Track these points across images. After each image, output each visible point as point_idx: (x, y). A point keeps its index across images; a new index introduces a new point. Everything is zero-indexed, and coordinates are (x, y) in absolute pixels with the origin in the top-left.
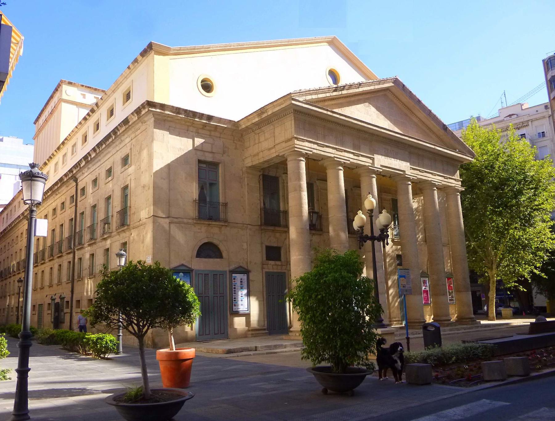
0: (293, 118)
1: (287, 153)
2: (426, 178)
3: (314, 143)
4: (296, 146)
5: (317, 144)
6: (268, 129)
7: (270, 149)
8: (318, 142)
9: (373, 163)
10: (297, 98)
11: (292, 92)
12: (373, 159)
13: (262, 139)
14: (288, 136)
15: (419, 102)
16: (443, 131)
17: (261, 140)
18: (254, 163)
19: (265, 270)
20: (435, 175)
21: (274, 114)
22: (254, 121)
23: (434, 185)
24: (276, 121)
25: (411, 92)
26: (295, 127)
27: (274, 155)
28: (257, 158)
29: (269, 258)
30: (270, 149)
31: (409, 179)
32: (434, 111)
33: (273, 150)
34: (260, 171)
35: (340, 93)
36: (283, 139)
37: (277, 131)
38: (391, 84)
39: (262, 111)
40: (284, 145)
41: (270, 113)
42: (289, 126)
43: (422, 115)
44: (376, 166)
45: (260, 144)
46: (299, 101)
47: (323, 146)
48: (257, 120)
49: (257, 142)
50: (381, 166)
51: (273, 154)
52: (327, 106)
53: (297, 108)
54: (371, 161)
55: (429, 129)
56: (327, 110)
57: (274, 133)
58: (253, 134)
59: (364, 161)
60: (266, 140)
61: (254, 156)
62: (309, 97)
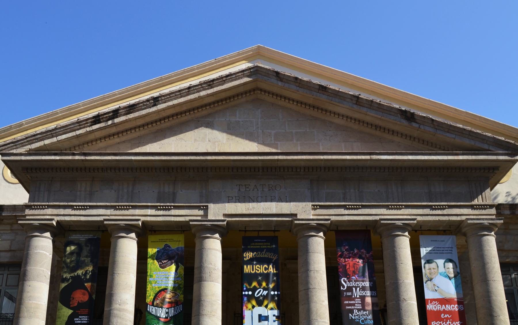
3: (65, 207)
4: (27, 217)
5: (72, 207)
9: (206, 215)
10: (14, 151)
16: (405, 122)
20: (399, 208)
35: (110, 122)
43: (343, 109)
44: (210, 217)
47: (85, 208)
50: (225, 215)
52: (106, 148)
54: (201, 212)
55: (377, 127)
56: (74, 154)
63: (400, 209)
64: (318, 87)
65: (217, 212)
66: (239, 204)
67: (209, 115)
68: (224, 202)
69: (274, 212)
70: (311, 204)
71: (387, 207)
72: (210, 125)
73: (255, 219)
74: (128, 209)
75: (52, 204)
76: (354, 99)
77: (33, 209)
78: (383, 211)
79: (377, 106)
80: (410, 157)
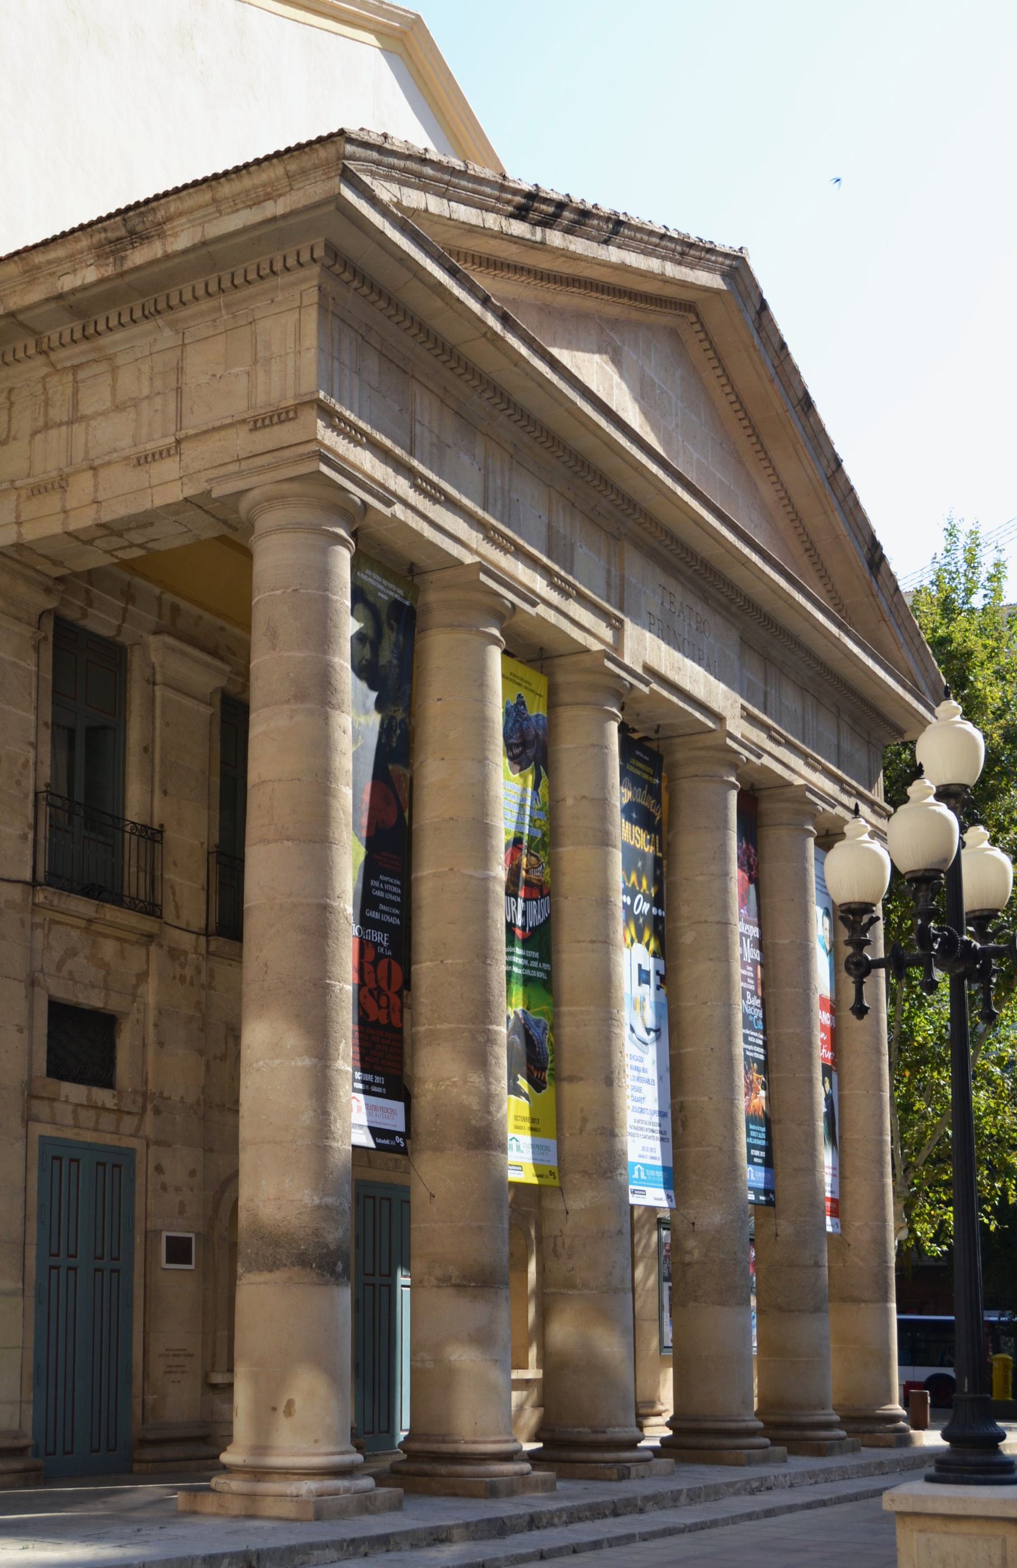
0: (313, 296)
1: (261, 484)
2: (786, 774)
6: (138, 353)
7: (143, 460)
8: (415, 463)
9: (618, 644)
11: (352, 127)
12: (618, 628)
13: (95, 398)
14: (276, 387)
15: (806, 404)
16: (867, 573)
17: (87, 407)
18: (30, 534)
19: (41, 1129)
21: (208, 256)
22: (68, 283)
23: (813, 814)
24: (204, 305)
25: (783, 346)
26: (320, 349)
27: (175, 494)
28: (53, 502)
29: (60, 1068)
30: (143, 460)
31: (734, 763)
32: (850, 469)
33: (169, 468)
34: (48, 591)
36: (239, 407)
37: (200, 364)
38: (713, 280)
39: (134, 223)
40: (242, 441)
41: (182, 241)
42: (287, 340)
45: (79, 429)
46: (373, 200)
48: (91, 275)
49: (59, 412)
51: (167, 485)
53: (351, 244)
54: (608, 634)
57: (180, 370)
58: (38, 368)
59: (584, 627)
60: (118, 408)
61: (37, 491)
62: (414, 198)
63: (815, 769)
64: (800, 395)
65: (644, 648)
66: (664, 646)
67: (615, 323)
68: (644, 627)
69: (699, 692)
70: (742, 701)
71: (805, 756)
72: (617, 361)
73: (674, 699)
74: (506, 551)
75: (379, 436)
76: (833, 466)
77: (334, 428)
78: (797, 763)
79: (851, 504)
80: (870, 662)
